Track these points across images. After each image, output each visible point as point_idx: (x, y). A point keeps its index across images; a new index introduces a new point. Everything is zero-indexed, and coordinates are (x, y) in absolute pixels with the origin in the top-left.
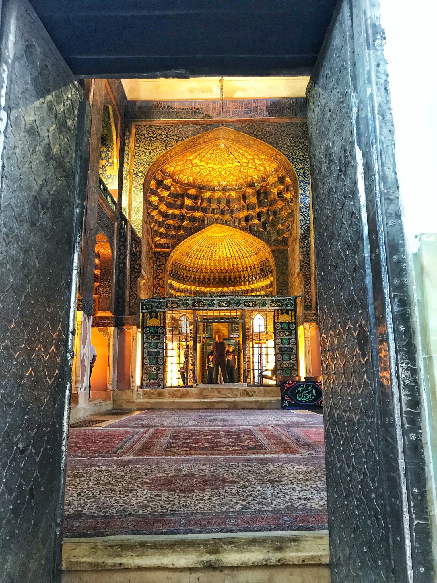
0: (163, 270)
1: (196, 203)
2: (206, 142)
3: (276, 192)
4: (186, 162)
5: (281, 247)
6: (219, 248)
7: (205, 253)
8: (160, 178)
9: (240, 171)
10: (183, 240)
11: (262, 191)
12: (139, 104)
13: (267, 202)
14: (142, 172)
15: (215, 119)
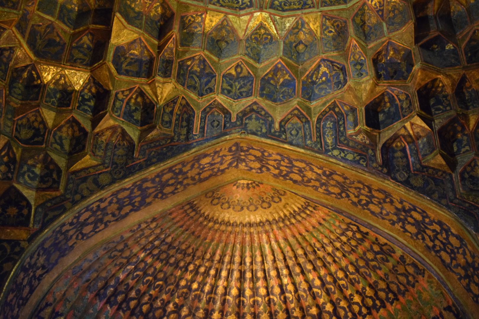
6: (242, 278)
7: (185, 296)
10: (92, 193)
13: (453, 52)
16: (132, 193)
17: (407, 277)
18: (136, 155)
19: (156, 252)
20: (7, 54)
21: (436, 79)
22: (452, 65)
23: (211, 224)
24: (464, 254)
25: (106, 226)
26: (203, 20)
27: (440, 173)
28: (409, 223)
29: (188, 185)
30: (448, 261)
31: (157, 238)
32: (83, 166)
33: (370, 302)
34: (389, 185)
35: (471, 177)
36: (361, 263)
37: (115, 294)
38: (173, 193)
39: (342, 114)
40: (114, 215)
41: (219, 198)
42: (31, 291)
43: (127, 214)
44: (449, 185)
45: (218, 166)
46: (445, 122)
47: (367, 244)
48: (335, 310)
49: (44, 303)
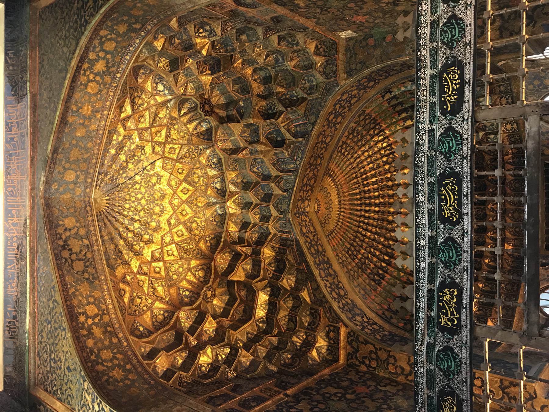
0: (389, 356)
1: (247, 256)
2: (88, 233)
3: (210, 78)
4: (145, 274)
5: (341, 58)
6: (370, 205)
8: (168, 336)
9: (177, 160)
10: (321, 292)
11: (222, 113)
12: (9, 369)
13: (244, 101)
14: (93, 402)
15: (28, 214)
16: (321, 269)
17: (367, 119)
18: (301, 268)
19: (355, 253)
20: (250, 336)
21: (258, 110)
22: (251, 102)
23: (340, 224)
24: (352, 91)
25: (340, 282)
26: (232, 231)
27: (308, 106)
28: (336, 121)
29: (318, 238)
30: (356, 99)
31: (347, 252)
32: (307, 296)
33: (382, 137)
34: (314, 133)
35: (309, 89)
36: (360, 144)
37: (378, 275)
38: (322, 246)
39: (278, 159)
40: (334, 278)
41: (325, 220)
42: (376, 324)
43: (334, 271)
44: (314, 101)
45: (307, 223)
46: (280, 105)
47: (349, 141)
48: (386, 156)
49: (383, 316)
